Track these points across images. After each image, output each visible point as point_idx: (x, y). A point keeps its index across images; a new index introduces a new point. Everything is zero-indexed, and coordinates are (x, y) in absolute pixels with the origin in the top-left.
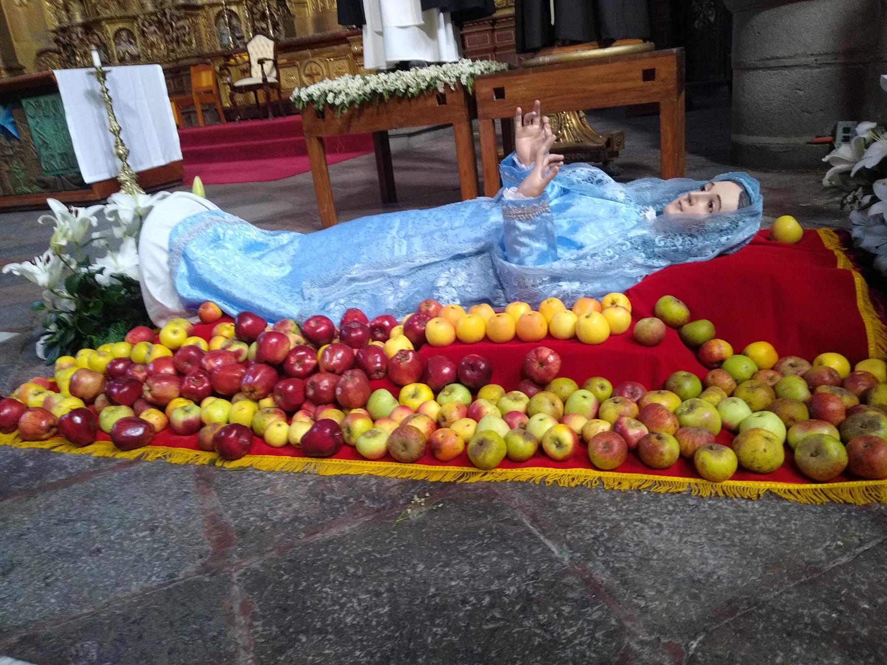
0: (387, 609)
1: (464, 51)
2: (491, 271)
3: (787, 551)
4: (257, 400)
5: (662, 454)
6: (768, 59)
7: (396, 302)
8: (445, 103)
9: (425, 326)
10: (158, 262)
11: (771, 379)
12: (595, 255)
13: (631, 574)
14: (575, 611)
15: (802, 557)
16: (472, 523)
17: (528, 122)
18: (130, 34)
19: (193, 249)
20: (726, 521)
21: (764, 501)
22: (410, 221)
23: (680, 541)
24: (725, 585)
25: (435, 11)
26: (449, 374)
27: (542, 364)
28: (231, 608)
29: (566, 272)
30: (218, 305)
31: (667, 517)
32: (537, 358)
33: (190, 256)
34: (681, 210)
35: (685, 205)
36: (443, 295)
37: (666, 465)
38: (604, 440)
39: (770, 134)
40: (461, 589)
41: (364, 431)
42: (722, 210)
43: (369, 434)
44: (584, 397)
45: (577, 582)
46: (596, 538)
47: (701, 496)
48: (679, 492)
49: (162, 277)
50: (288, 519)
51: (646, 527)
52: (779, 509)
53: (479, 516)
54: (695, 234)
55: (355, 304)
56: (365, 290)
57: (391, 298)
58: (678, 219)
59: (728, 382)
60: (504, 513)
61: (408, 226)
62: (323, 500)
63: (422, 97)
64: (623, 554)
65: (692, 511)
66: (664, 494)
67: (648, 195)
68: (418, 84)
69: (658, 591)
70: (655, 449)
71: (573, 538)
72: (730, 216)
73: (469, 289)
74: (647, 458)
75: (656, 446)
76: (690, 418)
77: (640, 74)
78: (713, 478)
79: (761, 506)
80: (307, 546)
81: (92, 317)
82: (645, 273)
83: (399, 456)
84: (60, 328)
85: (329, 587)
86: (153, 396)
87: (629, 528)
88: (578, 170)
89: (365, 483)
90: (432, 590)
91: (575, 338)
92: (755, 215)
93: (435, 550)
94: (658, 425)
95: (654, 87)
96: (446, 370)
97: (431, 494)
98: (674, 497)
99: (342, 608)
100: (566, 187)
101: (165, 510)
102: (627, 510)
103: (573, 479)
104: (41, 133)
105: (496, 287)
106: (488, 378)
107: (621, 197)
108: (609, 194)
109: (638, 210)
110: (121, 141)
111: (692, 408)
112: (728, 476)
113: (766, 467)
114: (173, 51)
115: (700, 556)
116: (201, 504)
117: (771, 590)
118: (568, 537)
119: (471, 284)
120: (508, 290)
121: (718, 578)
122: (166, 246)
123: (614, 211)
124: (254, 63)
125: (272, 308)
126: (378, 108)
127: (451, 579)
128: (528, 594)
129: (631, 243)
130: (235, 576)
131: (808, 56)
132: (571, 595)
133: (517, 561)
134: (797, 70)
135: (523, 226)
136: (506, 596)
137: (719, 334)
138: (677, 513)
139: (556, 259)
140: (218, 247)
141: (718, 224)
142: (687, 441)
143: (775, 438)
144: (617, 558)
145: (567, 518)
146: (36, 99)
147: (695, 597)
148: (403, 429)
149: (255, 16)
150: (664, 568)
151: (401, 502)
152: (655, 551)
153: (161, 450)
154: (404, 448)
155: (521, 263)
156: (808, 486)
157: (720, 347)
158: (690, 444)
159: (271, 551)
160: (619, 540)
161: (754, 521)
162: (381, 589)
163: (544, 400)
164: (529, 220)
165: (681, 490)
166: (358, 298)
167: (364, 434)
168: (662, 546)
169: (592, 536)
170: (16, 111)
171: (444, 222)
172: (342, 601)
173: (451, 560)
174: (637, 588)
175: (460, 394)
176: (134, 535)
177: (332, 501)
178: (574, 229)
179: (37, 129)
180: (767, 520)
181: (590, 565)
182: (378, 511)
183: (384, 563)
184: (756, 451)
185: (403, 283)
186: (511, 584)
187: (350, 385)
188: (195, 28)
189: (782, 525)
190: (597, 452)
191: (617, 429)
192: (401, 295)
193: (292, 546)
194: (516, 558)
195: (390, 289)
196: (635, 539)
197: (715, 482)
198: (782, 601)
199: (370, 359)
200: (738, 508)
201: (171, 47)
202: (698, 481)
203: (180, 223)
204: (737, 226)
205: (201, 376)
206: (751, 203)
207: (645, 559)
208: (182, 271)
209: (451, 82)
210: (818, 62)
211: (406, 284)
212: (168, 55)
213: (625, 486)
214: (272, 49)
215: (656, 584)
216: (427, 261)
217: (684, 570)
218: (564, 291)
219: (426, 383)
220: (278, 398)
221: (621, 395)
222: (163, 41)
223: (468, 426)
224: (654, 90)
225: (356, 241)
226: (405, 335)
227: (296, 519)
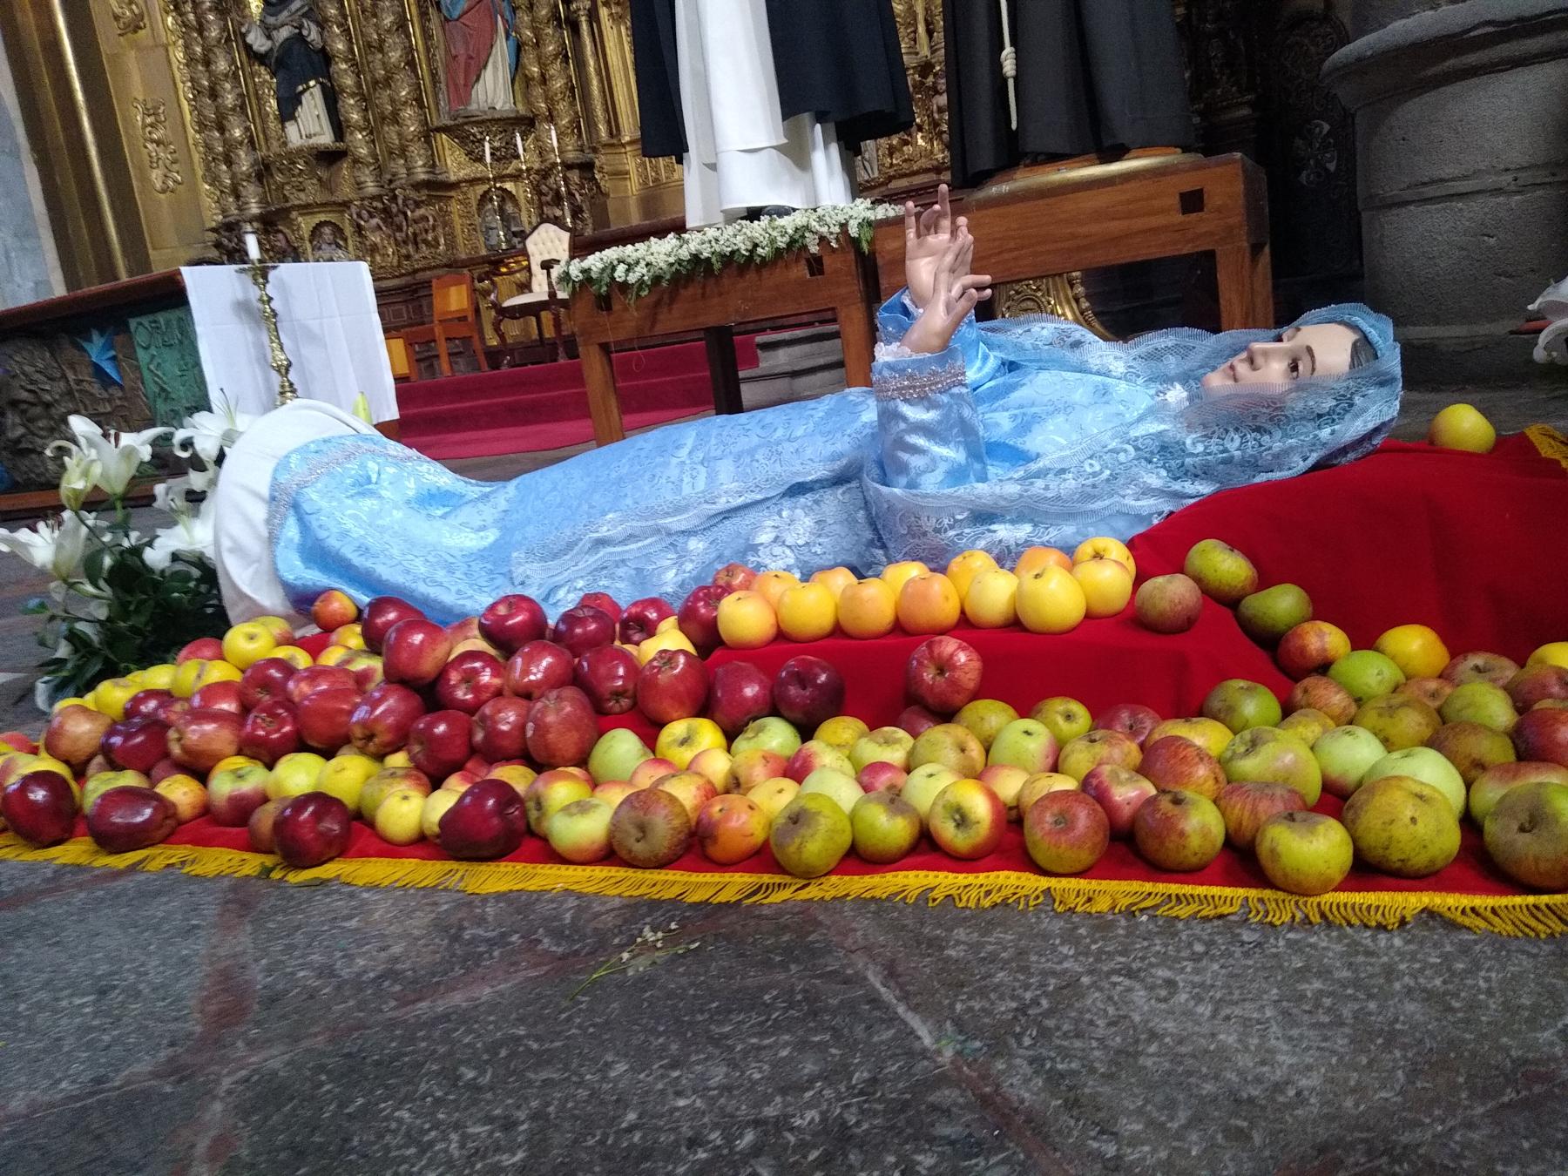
0: (520, 1155)
1: (858, 189)
2: (861, 513)
3: (1467, 1036)
4: (380, 757)
5: (1182, 834)
6: (1424, 184)
7: (680, 578)
8: (821, 272)
9: (716, 608)
10: (248, 520)
11: (1434, 695)
12: (1063, 471)
13: (1090, 1086)
14: (945, 1165)
15: (1506, 1049)
16: (754, 979)
17: (928, 228)
18: (338, 231)
19: (314, 496)
20: (1325, 973)
21: (1415, 931)
22: (714, 432)
23: (1214, 1016)
24: (1316, 1111)
25: (806, 117)
26: (755, 699)
27: (941, 671)
28: (193, 1146)
29: (1003, 503)
30: (350, 597)
31: (1189, 966)
32: (932, 658)
33: (306, 507)
34: (1236, 380)
35: (1242, 369)
36: (767, 561)
37: (1194, 860)
38: (1056, 809)
39: (1437, 321)
40: (697, 1113)
41: (567, 803)
42: (1316, 374)
43: (574, 810)
44: (1027, 733)
45: (961, 1100)
46: (1022, 1010)
47: (1271, 924)
48: (1221, 917)
49: (255, 547)
50: (372, 975)
51: (1137, 986)
52: (1448, 948)
53: (767, 965)
54: (1267, 426)
55: (603, 585)
56: (623, 561)
57: (671, 574)
58: (1228, 397)
59: (1338, 700)
60: (829, 959)
61: (708, 442)
62: (456, 938)
63: (780, 263)
64: (1078, 1044)
65: (1246, 955)
66: (1187, 921)
67: (1172, 363)
68: (773, 241)
69: (1151, 1123)
70: (1168, 823)
71: (971, 1009)
72: (1335, 386)
73: (818, 550)
74: (1151, 845)
75: (1168, 818)
76: (1250, 766)
77: (1175, 201)
78: (1298, 884)
79: (1408, 942)
80: (392, 1024)
81: (133, 629)
82: (1167, 507)
83: (630, 851)
84: (76, 651)
85: (410, 1109)
86: (185, 749)
87: (1101, 989)
88: (1036, 328)
89: (554, 906)
90: (632, 1116)
91: (1015, 624)
92: (1384, 382)
93: (660, 1034)
94: (1180, 778)
95: (1204, 224)
96: (750, 691)
97: (682, 927)
98: (1207, 925)
99: (423, 1152)
100: (1012, 358)
101: (143, 958)
102: (1101, 951)
103: (988, 893)
104: (159, 373)
105: (871, 544)
106: (834, 703)
107: (1119, 367)
108: (1094, 362)
109: (1152, 392)
110: (291, 385)
111: (1254, 745)
112: (1332, 880)
113: (1419, 860)
114: (408, 257)
115: (1259, 1047)
116: (215, 947)
117: (1428, 1121)
118: (959, 1007)
119: (821, 540)
120: (891, 545)
121: (1299, 1094)
122: (265, 491)
123: (1103, 393)
124: (536, 268)
125: (448, 598)
126: (704, 288)
127: (679, 1094)
128: (844, 1125)
129: (1137, 449)
130: (226, 1083)
131: (1499, 173)
132: (945, 1130)
133: (833, 1056)
134: (1481, 199)
135: (914, 413)
136: (791, 1129)
137: (1322, 610)
138: (1213, 959)
139: (983, 478)
140: (362, 494)
141: (1311, 403)
142: (1240, 810)
143: (1436, 795)
144: (1066, 1054)
145: (962, 971)
146: (151, 317)
147: (1241, 1136)
148: (641, 802)
149: (543, 198)
150: (1169, 1073)
151: (616, 941)
152: (1153, 1036)
153: (176, 853)
154: (640, 835)
155: (912, 485)
156: (1518, 900)
157: (1321, 635)
158: (1246, 814)
159: (316, 1035)
160: (1073, 1014)
161: (1390, 972)
162: (519, 1114)
163: (941, 737)
164: (924, 400)
165: (1225, 910)
166: (611, 577)
167: (566, 810)
168: (1170, 1025)
169: (1014, 1005)
170: (120, 339)
171: (775, 430)
172: (426, 1138)
173: (689, 1055)
174: (1101, 1115)
175: (776, 736)
176: (64, 1003)
177: (474, 940)
178: (1025, 425)
179: (152, 367)
180: (1422, 970)
181: (1000, 1065)
182: (563, 957)
183: (542, 1059)
184: (1392, 821)
185: (696, 545)
186: (809, 1105)
187: (551, 718)
188: (444, 220)
189: (1457, 980)
190: (1039, 835)
191: (1093, 790)
192: (689, 566)
193: (361, 1026)
194: (833, 1051)
195: (669, 556)
196: (1111, 1010)
197: (1307, 895)
198: (1452, 1145)
199: (602, 670)
200: (1354, 947)
201: (404, 251)
202: (1267, 894)
203: (295, 451)
204: (1351, 405)
205: (280, 711)
206: (1376, 357)
207: (1128, 1054)
208: (290, 534)
209: (831, 233)
210: (1520, 182)
211: (701, 545)
212: (399, 265)
213: (1102, 905)
214: (566, 246)
215: (1149, 1107)
216: (740, 501)
217: (1216, 1078)
218: (1000, 541)
219: (712, 718)
220: (416, 748)
221: (1108, 726)
222: (392, 242)
223: (780, 791)
224: (1203, 228)
225: (614, 475)
226: (681, 629)
227: (391, 974)
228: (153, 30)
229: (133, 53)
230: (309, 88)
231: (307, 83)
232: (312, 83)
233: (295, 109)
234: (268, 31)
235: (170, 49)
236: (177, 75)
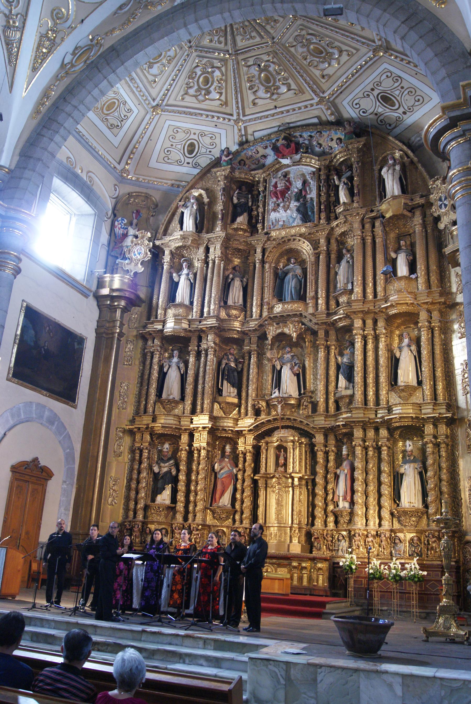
234: (160, 467)
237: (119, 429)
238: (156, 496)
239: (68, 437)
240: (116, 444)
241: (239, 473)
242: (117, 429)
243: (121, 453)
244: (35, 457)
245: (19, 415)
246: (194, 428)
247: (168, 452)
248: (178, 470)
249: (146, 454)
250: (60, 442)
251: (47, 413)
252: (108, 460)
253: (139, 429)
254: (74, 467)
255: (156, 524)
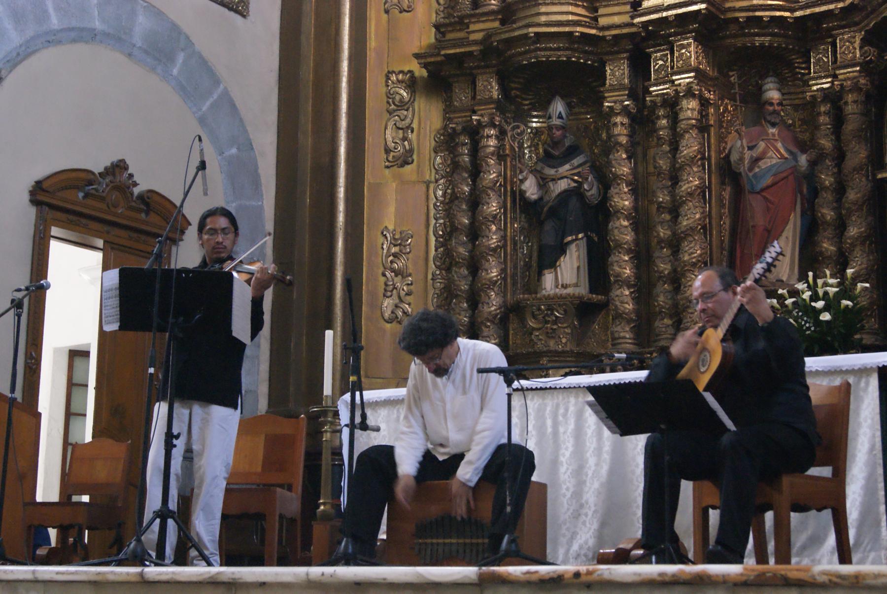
228: (419, 166)
229: (394, 185)
230: (577, 239)
231: (577, 235)
232: (580, 236)
233: (557, 259)
234: (543, 183)
235: (432, 186)
236: (432, 212)
237: (394, 78)
238: (540, 274)
239: (228, 104)
240: (390, 125)
241: (819, 167)
242: (388, 78)
243: (411, 151)
244: (115, 159)
245: (42, 16)
246: (645, 24)
247: (562, 128)
248: (606, 182)
249: (492, 142)
250: (202, 121)
251: (142, 23)
252: (369, 177)
253: (458, 60)
254: (261, 208)
255: (544, 361)
